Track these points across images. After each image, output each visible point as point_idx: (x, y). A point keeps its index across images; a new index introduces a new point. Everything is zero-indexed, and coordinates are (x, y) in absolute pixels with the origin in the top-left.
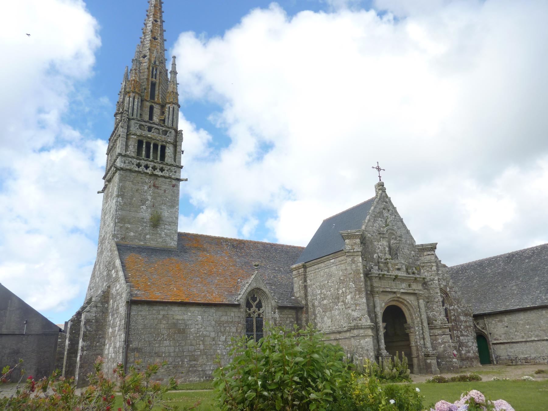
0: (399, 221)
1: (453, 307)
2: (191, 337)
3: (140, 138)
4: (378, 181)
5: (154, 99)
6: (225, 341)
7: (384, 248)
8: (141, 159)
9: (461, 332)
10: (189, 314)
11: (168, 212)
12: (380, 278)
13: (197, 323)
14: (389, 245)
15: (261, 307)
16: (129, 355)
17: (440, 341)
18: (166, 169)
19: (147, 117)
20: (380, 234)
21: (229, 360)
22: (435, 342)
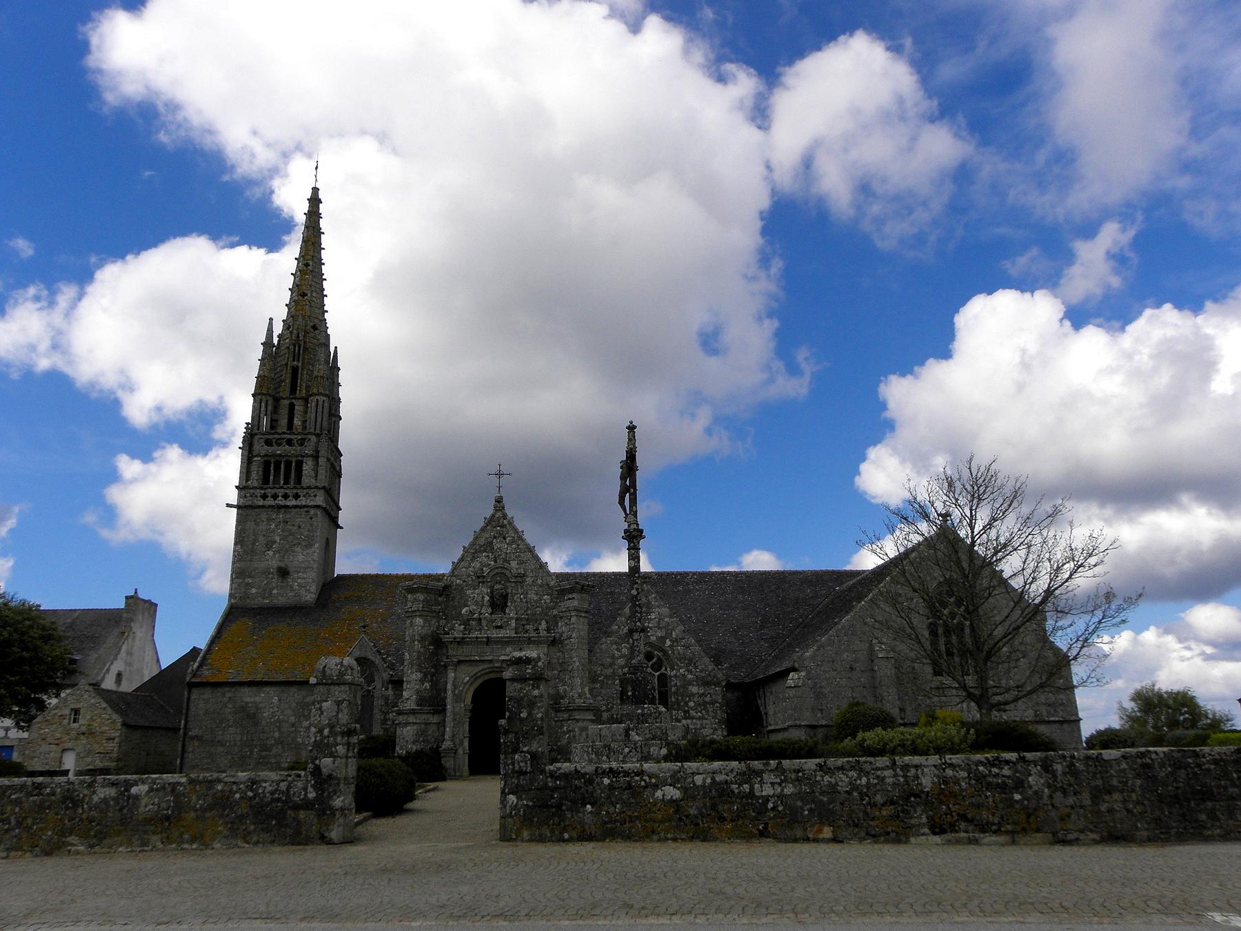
3: (266, 459)
5: (295, 394)
7: (483, 597)
8: (265, 489)
9: (688, 712)
14: (492, 592)
16: (187, 743)
18: (302, 495)
19: (284, 422)
20: (479, 577)
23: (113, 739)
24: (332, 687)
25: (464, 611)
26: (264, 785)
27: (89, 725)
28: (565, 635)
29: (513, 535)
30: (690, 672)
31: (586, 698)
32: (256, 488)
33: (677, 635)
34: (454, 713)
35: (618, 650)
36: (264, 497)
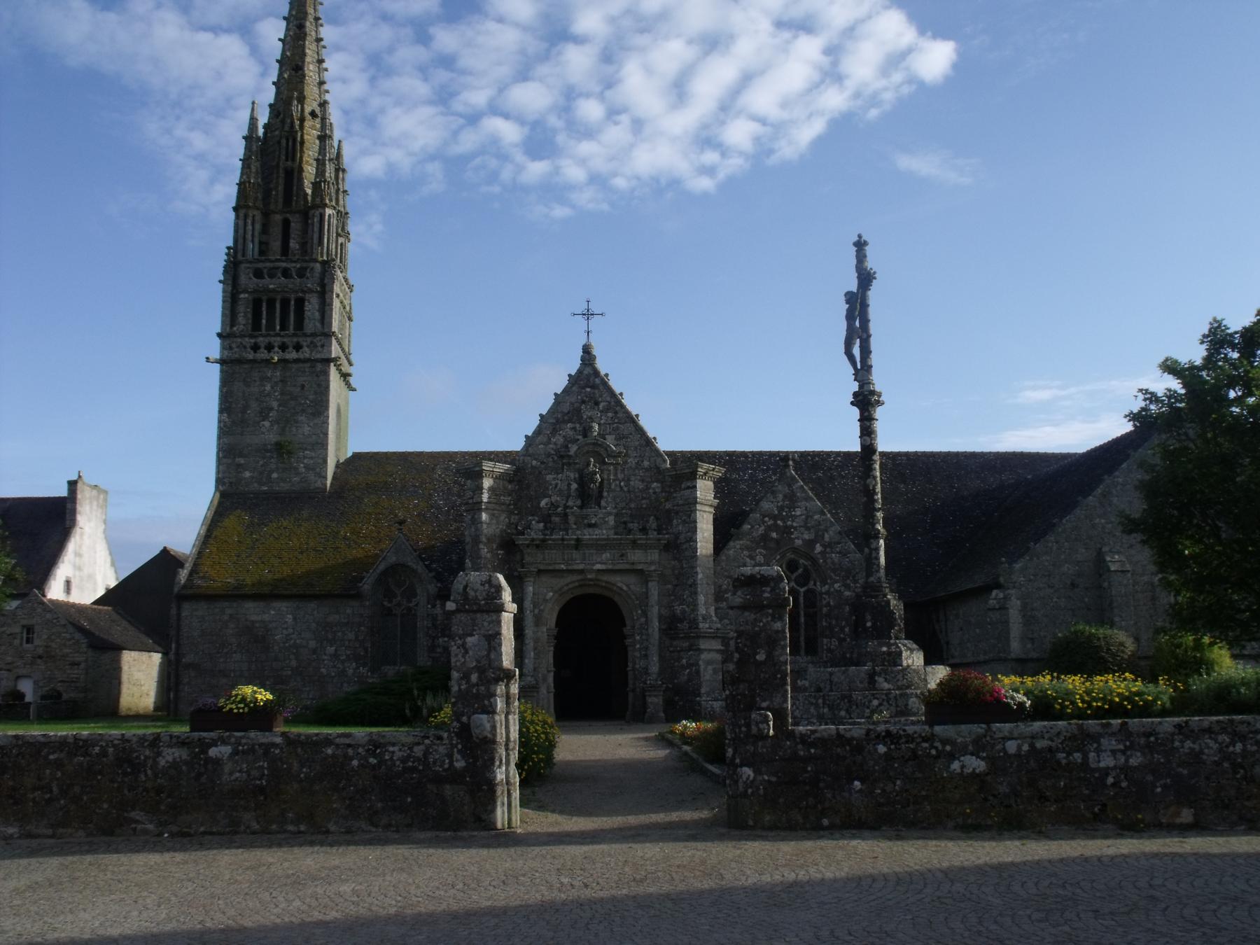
0: (626, 422)
1: (827, 586)
2: (276, 648)
4: (584, 342)
6: (335, 656)
7: (569, 485)
8: (256, 337)
10: (273, 612)
11: (309, 426)
12: (537, 546)
13: (285, 626)
15: (415, 595)
17: (684, 661)
18: (305, 344)
19: (276, 245)
20: (562, 457)
21: (342, 685)
22: (676, 664)
23: (78, 664)
24: (478, 615)
25: (543, 503)
26: (391, 749)
27: (47, 647)
28: (682, 537)
29: (608, 399)
30: (847, 587)
31: (712, 622)
32: (245, 336)
33: (830, 538)
34: (536, 641)
35: (751, 557)
36: (255, 348)
